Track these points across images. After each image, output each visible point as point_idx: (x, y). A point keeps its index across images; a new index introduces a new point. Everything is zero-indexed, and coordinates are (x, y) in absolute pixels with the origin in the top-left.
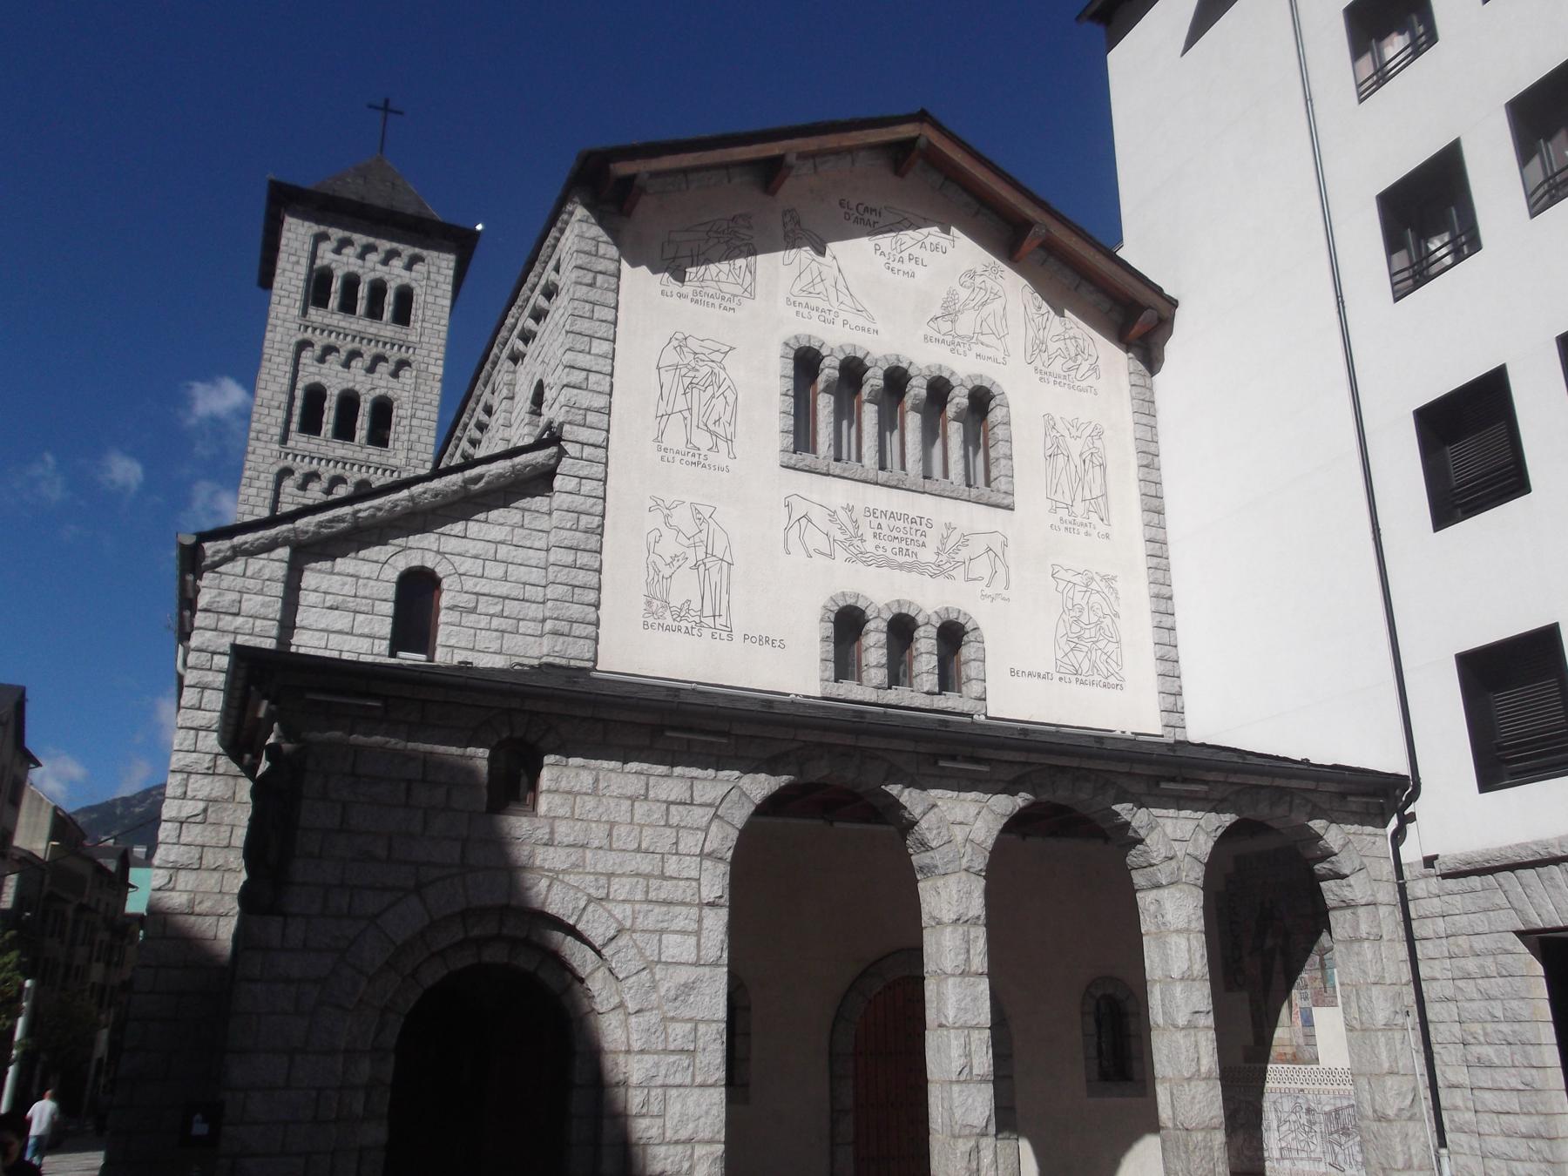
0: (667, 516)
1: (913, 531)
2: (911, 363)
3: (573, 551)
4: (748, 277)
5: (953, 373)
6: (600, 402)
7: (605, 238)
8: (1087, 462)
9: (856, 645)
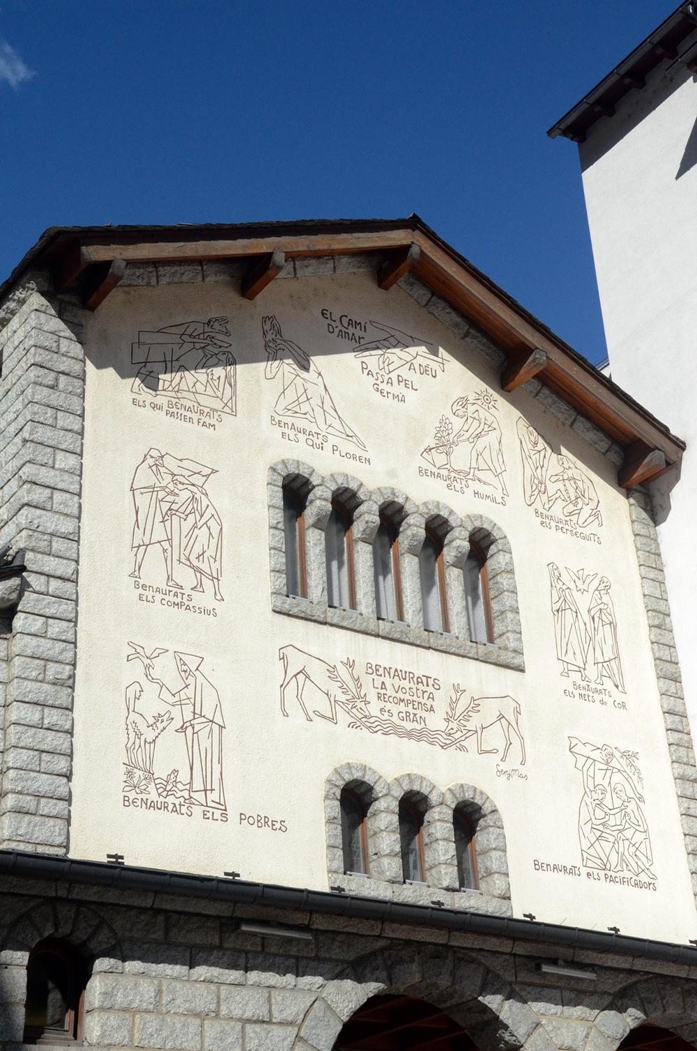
0: (147, 667)
1: (420, 693)
2: (407, 498)
3: (40, 708)
4: (228, 390)
5: (451, 512)
6: (67, 526)
7: (68, 333)
8: (596, 619)
9: (360, 828)
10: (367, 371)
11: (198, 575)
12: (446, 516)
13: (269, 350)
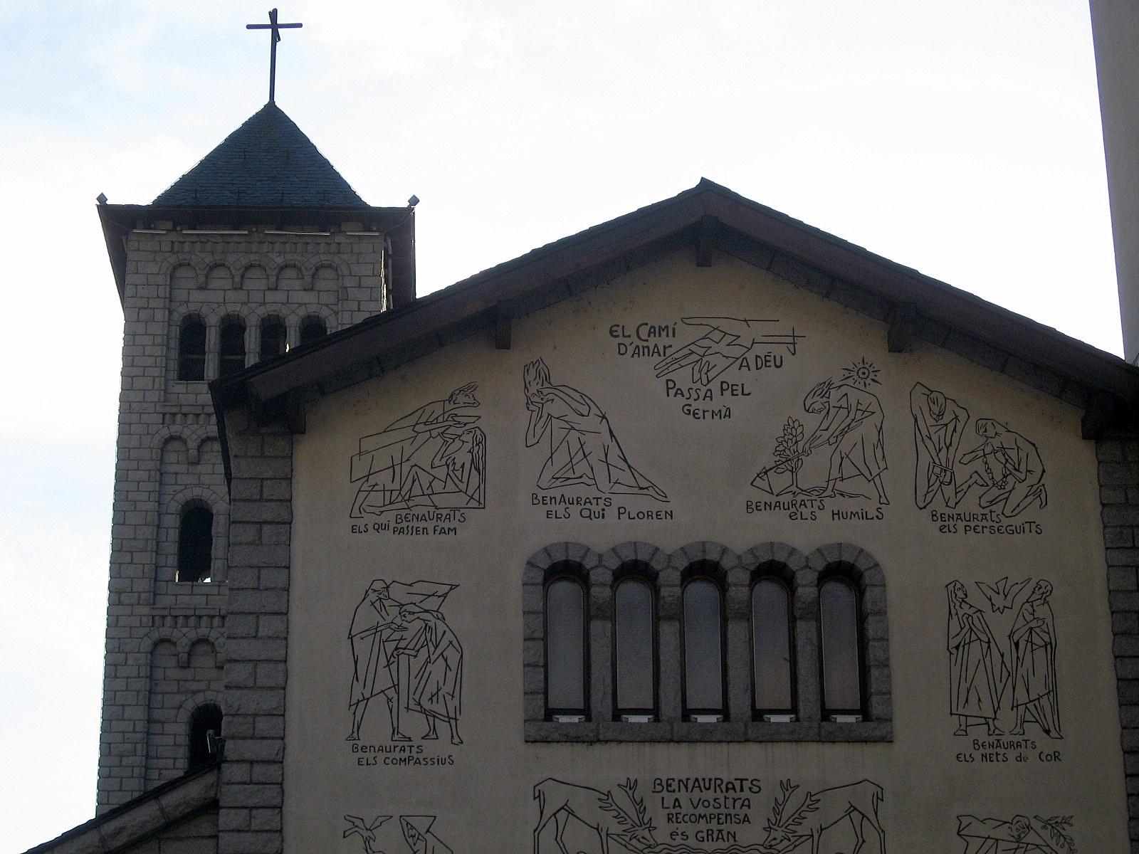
0: (367, 841)
1: (729, 803)
6: (269, 702)
8: (1022, 646)
10: (675, 390)
11: (431, 719)
12: (783, 560)
13: (532, 407)
